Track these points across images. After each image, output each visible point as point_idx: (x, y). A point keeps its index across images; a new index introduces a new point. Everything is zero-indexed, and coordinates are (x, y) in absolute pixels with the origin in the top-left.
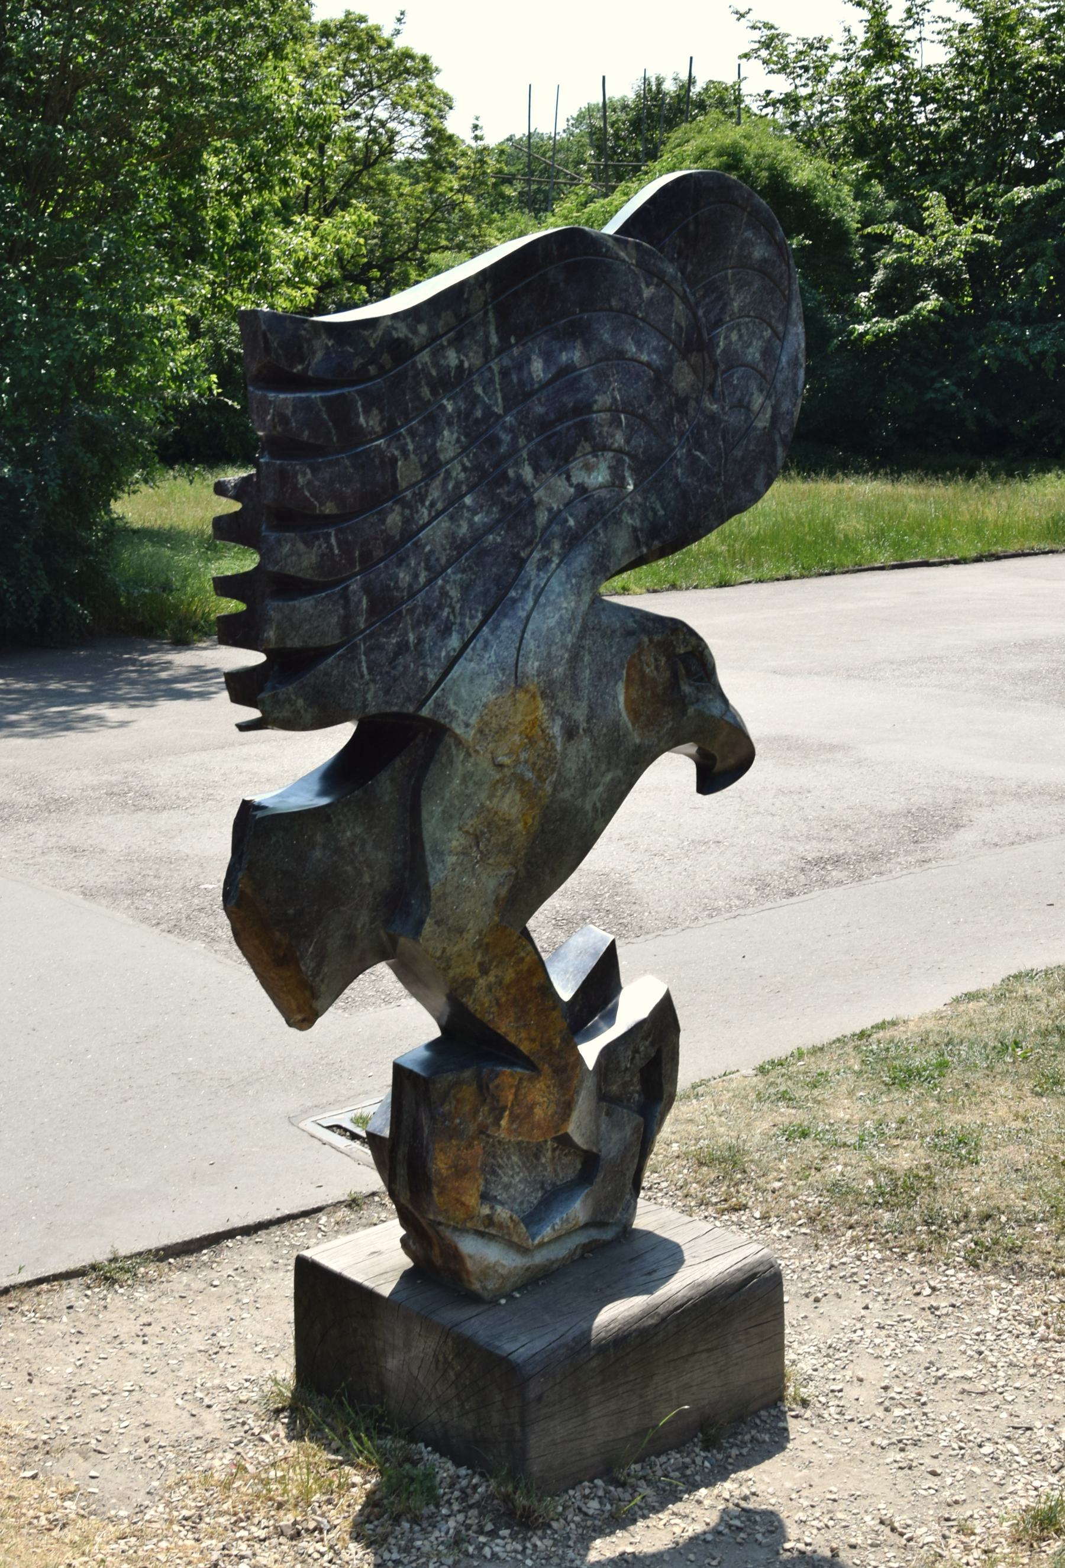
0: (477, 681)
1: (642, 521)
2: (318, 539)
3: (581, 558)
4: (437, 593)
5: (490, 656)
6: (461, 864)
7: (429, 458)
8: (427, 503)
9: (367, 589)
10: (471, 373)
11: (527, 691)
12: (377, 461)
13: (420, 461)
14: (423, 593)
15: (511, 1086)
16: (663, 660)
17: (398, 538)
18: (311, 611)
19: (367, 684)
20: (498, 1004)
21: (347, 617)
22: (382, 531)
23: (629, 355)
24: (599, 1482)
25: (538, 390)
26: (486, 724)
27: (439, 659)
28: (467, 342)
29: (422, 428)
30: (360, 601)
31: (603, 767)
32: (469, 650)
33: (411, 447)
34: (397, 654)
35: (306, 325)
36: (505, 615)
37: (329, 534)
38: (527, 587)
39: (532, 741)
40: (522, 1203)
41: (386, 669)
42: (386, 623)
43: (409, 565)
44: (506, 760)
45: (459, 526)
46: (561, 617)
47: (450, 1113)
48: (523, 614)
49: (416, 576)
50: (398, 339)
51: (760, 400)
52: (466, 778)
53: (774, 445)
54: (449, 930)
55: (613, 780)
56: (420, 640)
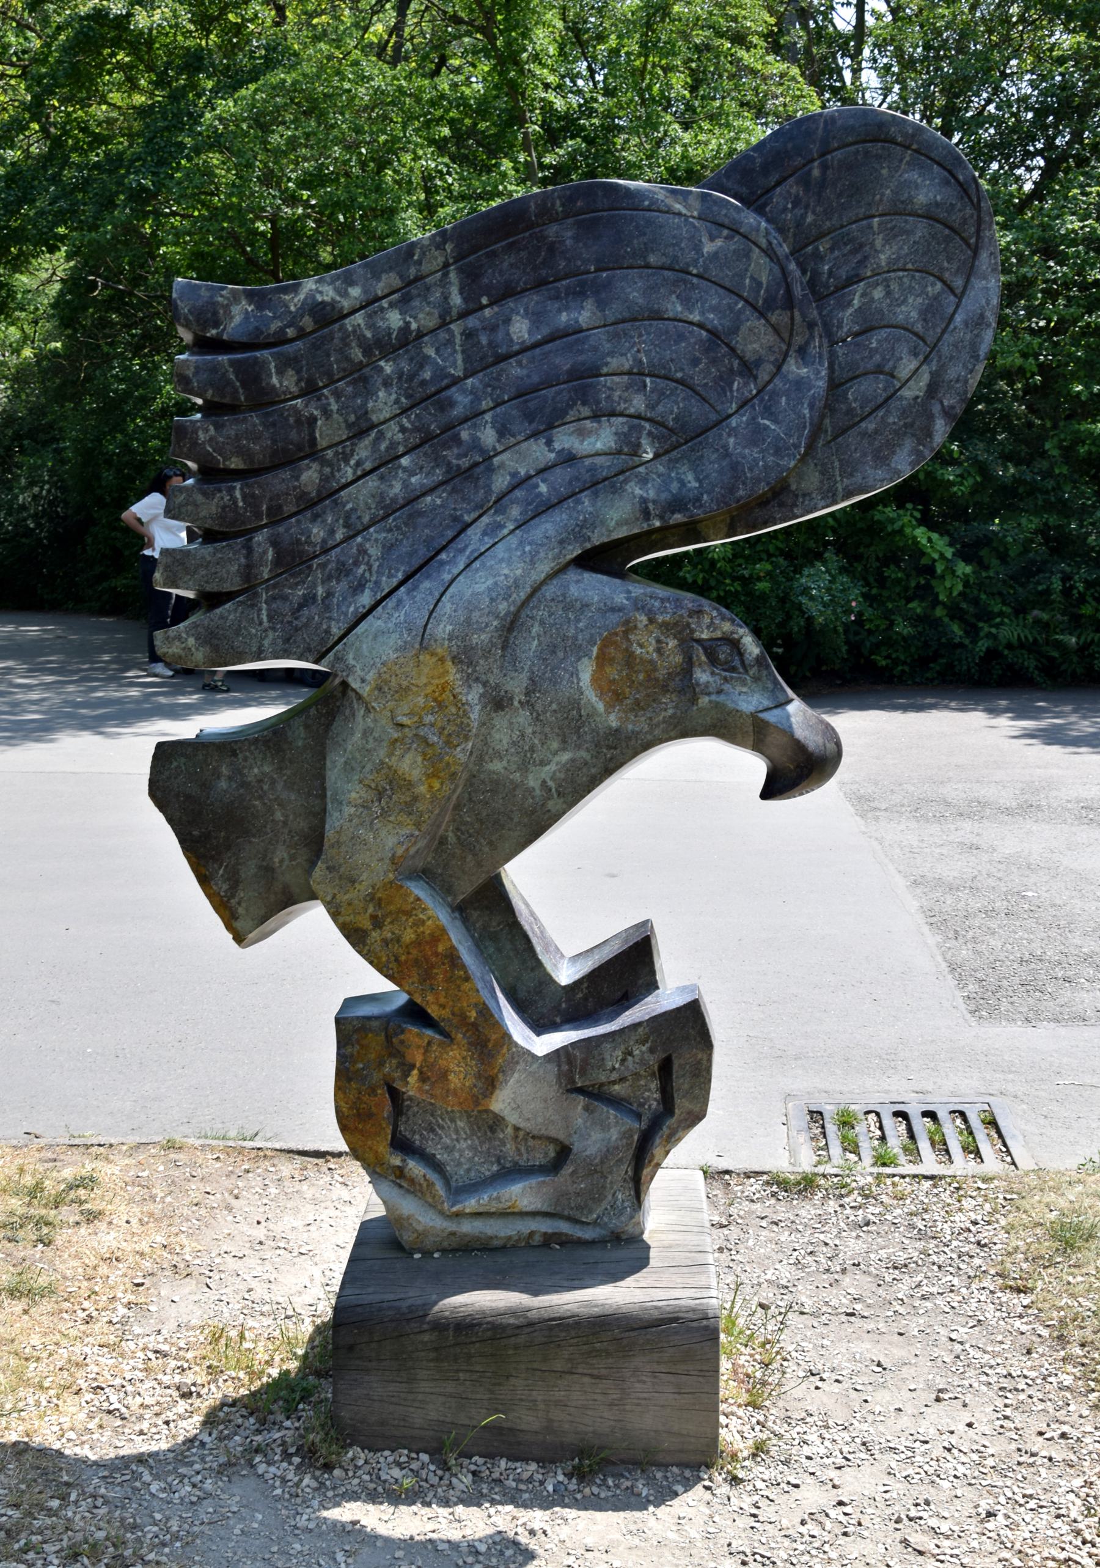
0: (380, 639)
1: (659, 491)
2: (220, 491)
3: (548, 526)
4: (354, 550)
5: (400, 616)
6: (359, 817)
7: (358, 418)
8: (352, 462)
9: (274, 543)
10: (420, 335)
11: (433, 654)
12: (291, 420)
13: (346, 421)
14: (338, 550)
15: (419, 1047)
16: (672, 643)
17: (314, 494)
18: (208, 558)
19: (266, 631)
20: (397, 960)
21: (249, 566)
22: (295, 488)
23: (671, 315)
24: (425, 1457)
25: (518, 353)
26: (386, 682)
27: (346, 614)
28: (416, 303)
29: (350, 389)
30: (265, 552)
31: (555, 745)
32: (380, 608)
33: (334, 407)
34: (301, 606)
35: (224, 292)
36: (428, 577)
37: (234, 488)
38: (462, 551)
39: (441, 706)
40: (468, 1170)
41: (288, 618)
42: (292, 575)
43: (324, 521)
44: (405, 720)
45: (391, 486)
46: (496, 583)
47: (352, 1056)
48: (447, 577)
49: (332, 532)
50: (323, 302)
51: (913, 365)
52: (366, 733)
53: (931, 417)
54: (341, 878)
55: (573, 760)
56: (329, 594)
